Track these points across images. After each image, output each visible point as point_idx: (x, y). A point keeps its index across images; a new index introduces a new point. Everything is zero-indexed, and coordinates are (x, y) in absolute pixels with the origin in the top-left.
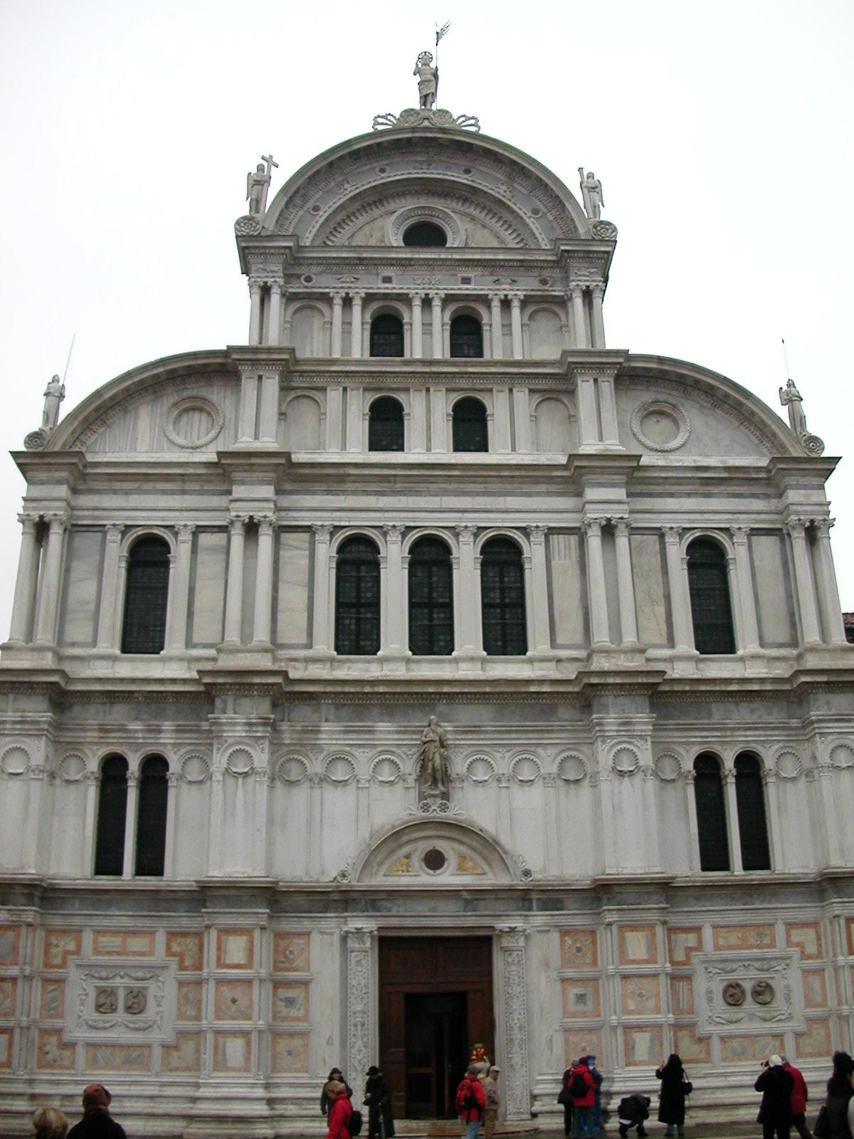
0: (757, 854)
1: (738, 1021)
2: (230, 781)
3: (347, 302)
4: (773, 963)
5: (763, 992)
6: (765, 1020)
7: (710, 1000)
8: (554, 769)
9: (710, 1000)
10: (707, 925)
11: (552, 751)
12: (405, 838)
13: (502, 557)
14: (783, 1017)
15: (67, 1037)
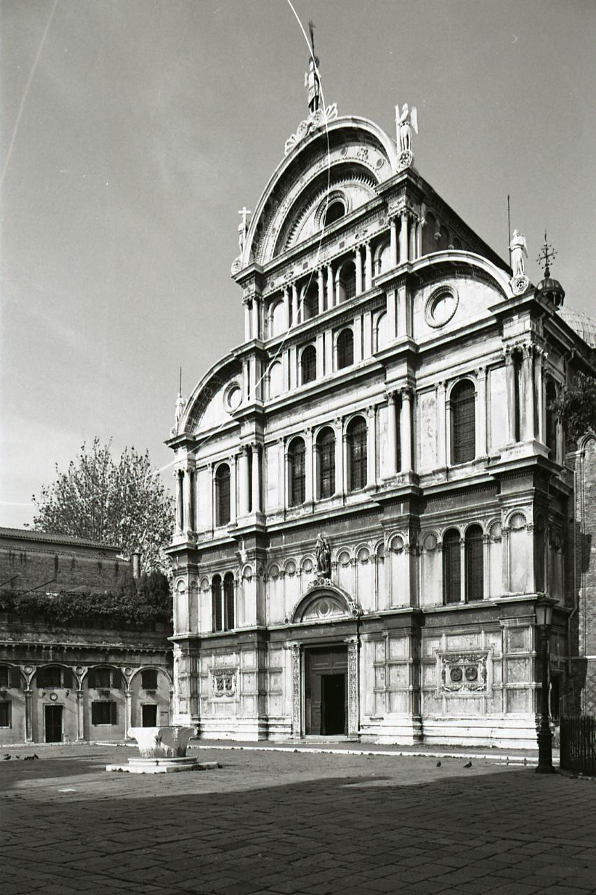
0: (475, 589)
1: (457, 690)
2: (245, 580)
3: (290, 290)
4: (479, 656)
5: (472, 674)
6: (471, 690)
7: (444, 678)
8: (376, 553)
9: (444, 678)
10: (444, 635)
11: (375, 542)
12: (314, 597)
13: (356, 427)
14: (481, 689)
15: (210, 700)
